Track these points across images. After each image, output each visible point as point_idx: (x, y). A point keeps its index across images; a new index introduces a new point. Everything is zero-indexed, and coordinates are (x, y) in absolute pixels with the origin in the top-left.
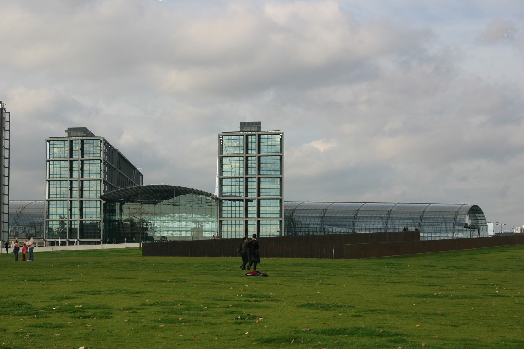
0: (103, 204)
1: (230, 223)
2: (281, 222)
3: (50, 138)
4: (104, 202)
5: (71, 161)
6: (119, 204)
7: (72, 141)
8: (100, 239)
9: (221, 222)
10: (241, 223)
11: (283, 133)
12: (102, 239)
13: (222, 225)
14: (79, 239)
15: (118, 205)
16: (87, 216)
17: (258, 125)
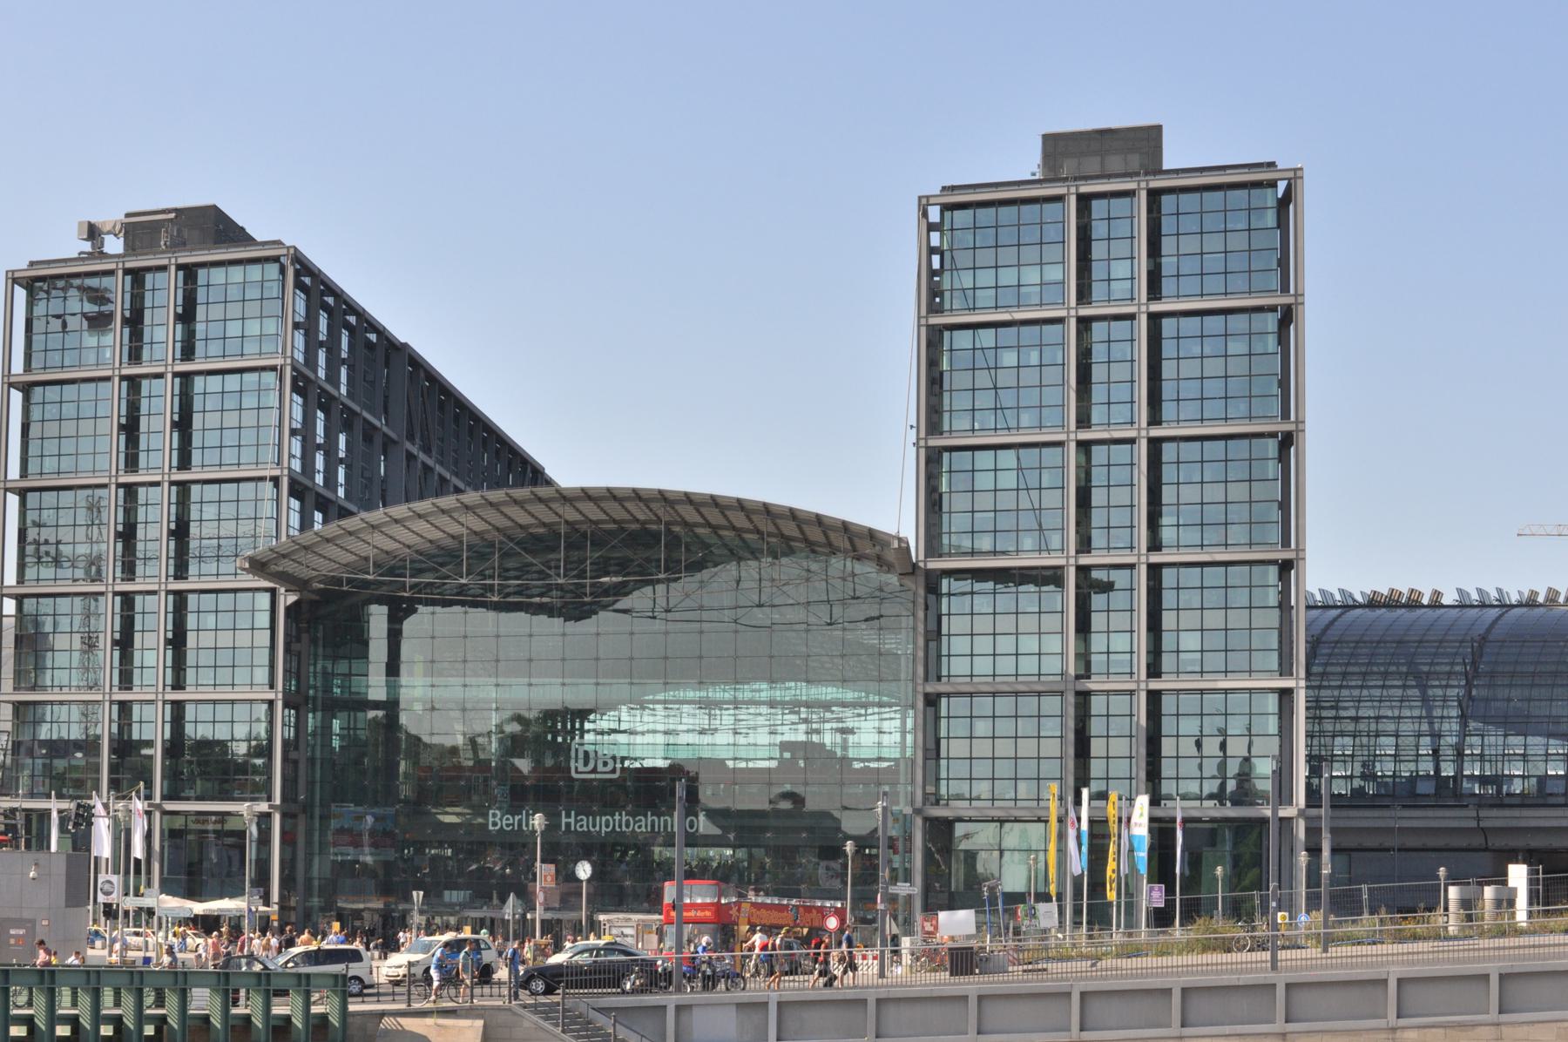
0: (288, 609)
1: (983, 705)
2: (1285, 694)
3: (32, 264)
4: (292, 598)
5: (133, 382)
6: (384, 609)
7: (137, 275)
8: (269, 799)
9: (932, 701)
10: (1051, 704)
11: (1295, 177)
12: (278, 801)
13: (937, 718)
14: (164, 798)
15: (378, 619)
16: (206, 676)
17: (1147, 140)
